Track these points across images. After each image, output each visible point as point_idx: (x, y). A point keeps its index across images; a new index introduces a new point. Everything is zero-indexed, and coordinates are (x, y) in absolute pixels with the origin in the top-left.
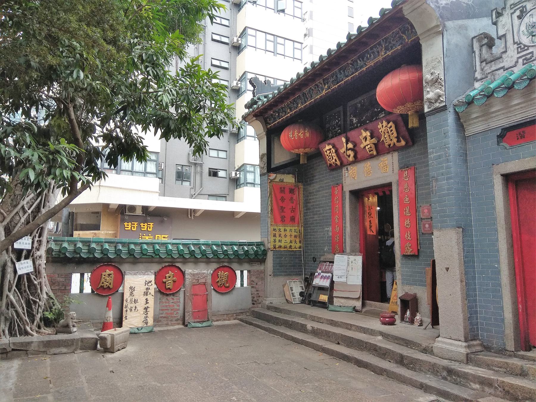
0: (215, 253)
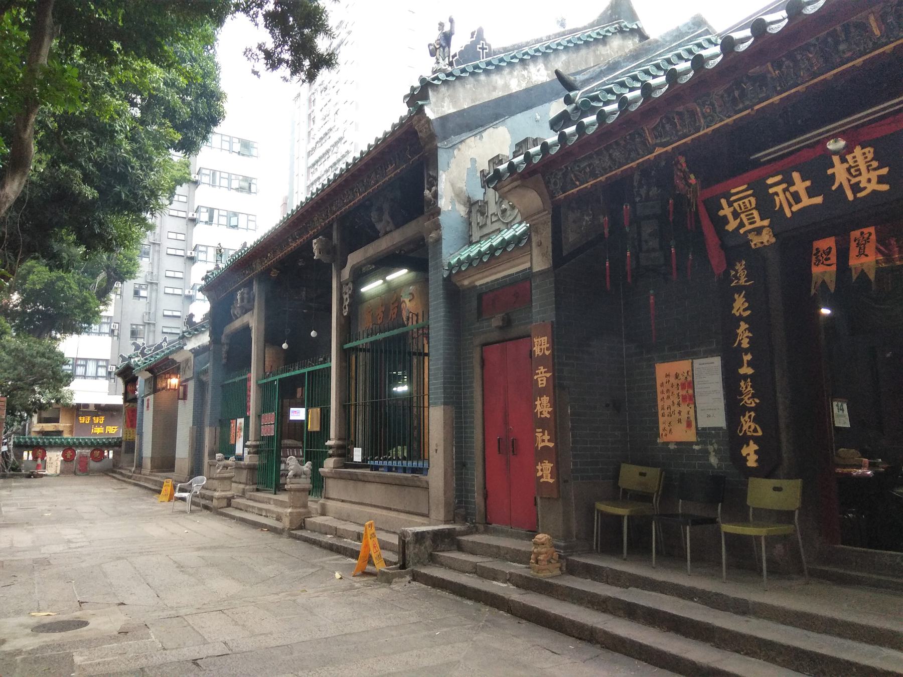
0: (92, 443)
